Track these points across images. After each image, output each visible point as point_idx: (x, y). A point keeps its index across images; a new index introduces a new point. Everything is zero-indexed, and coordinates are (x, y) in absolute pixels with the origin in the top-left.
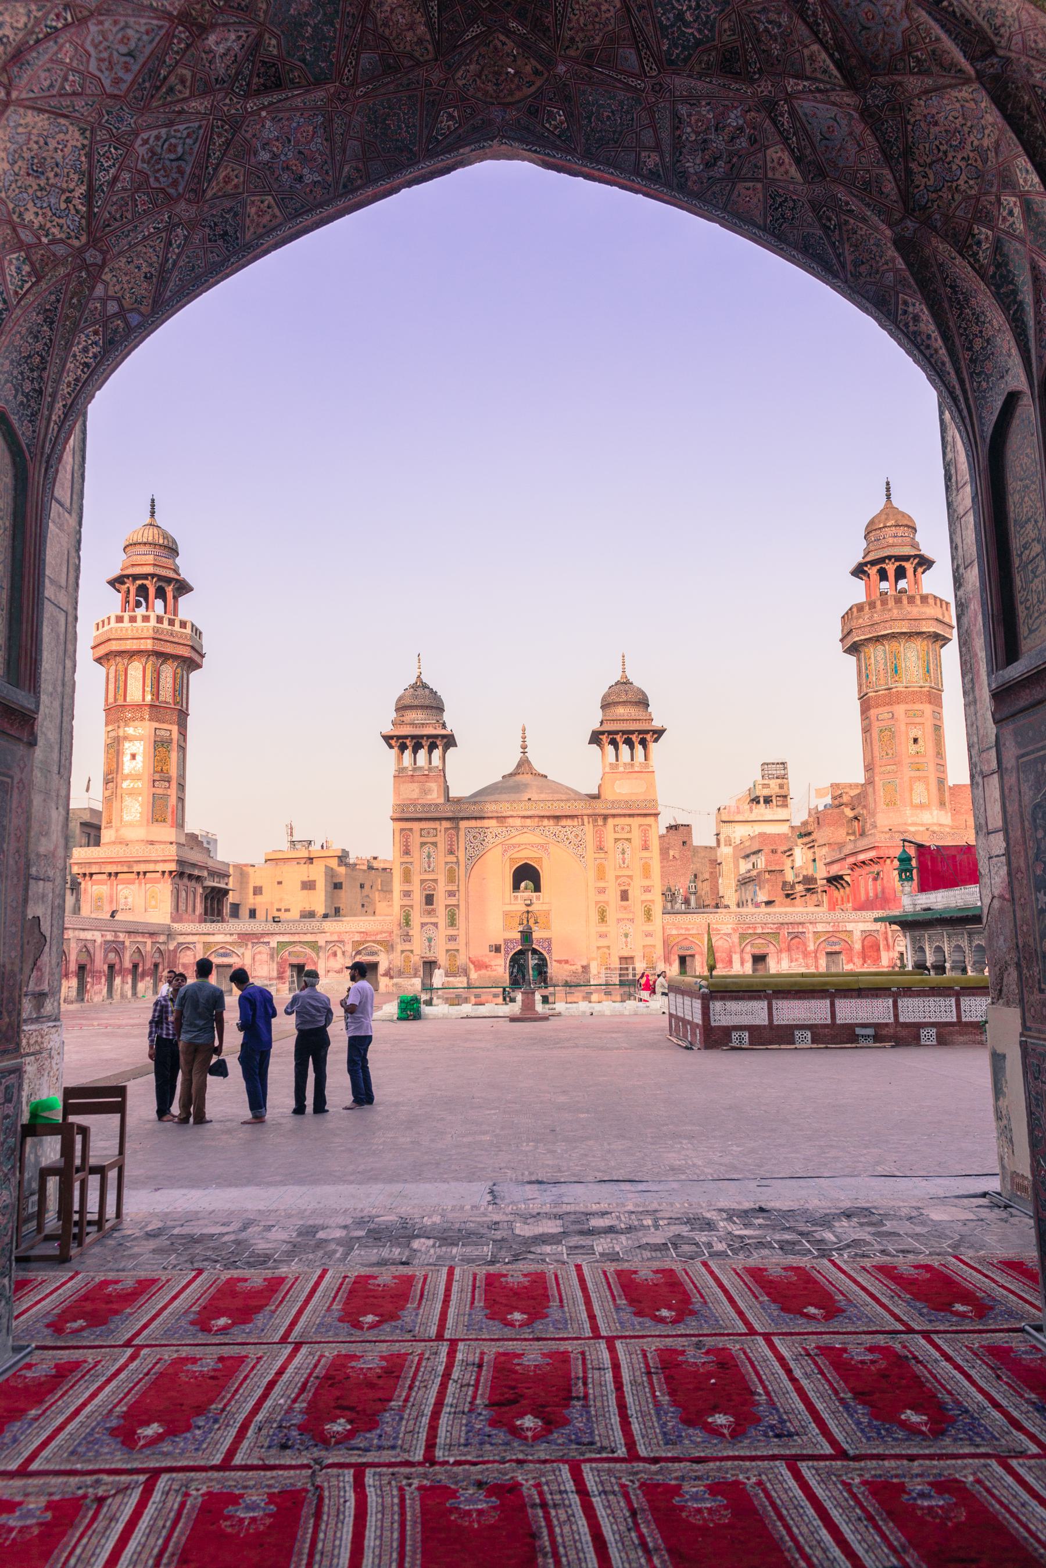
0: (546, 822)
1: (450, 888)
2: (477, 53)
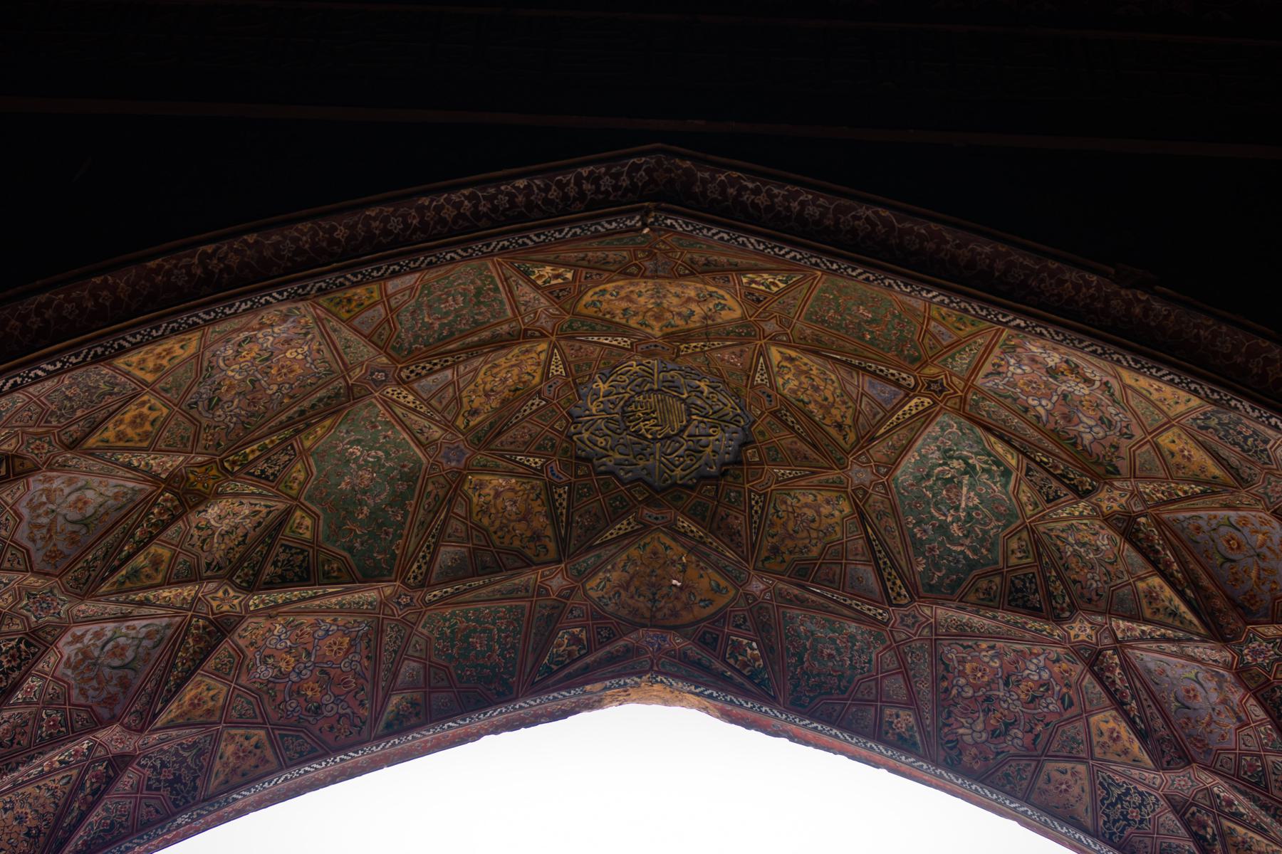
2: (624, 556)
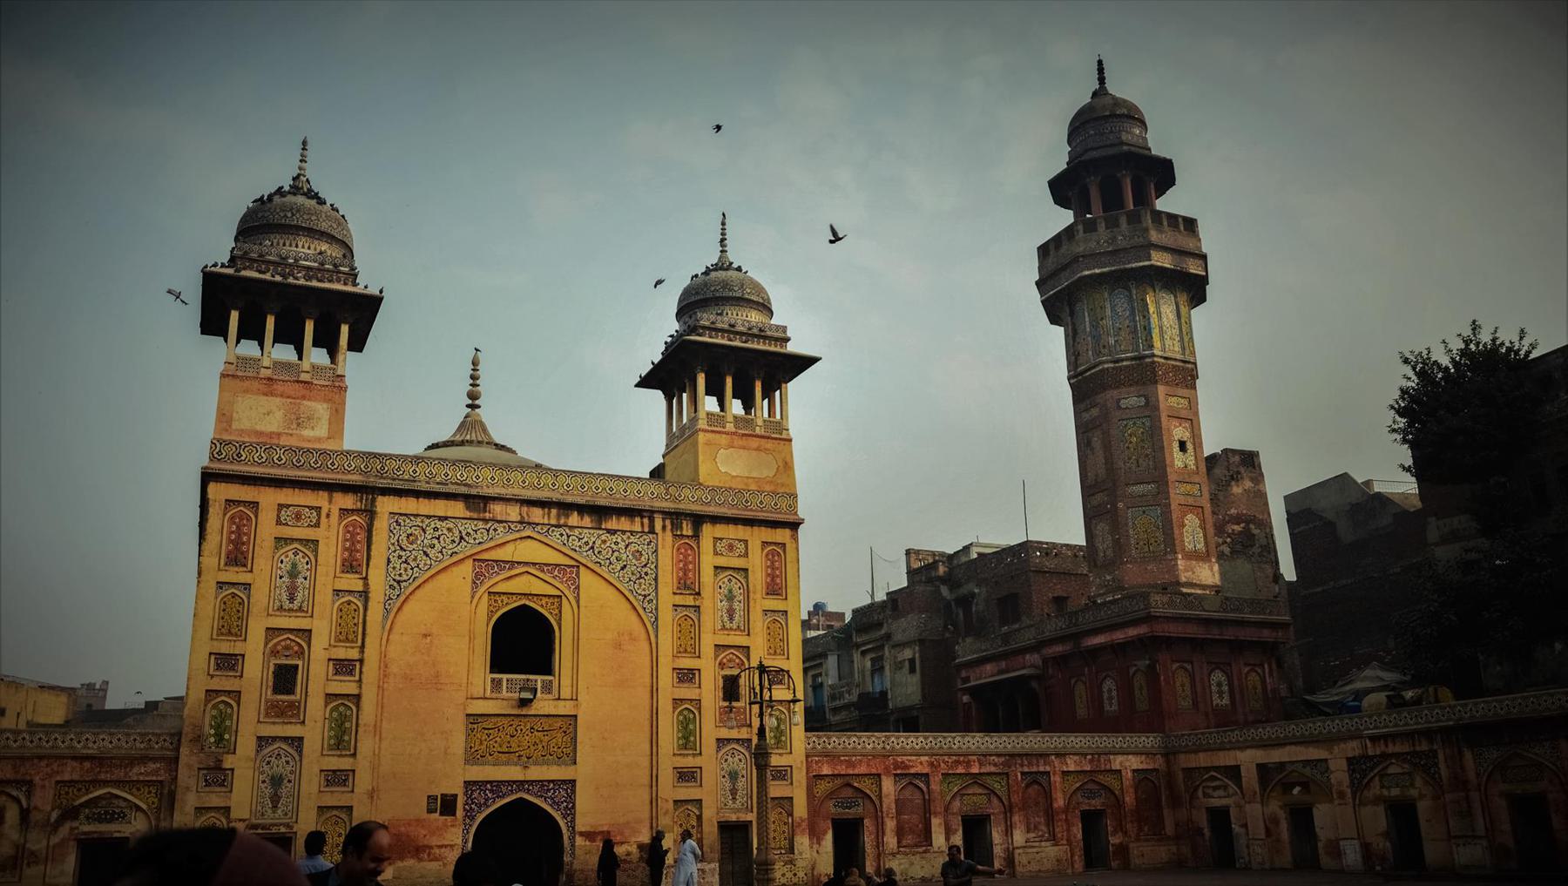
0: (574, 519)
1: (341, 653)
